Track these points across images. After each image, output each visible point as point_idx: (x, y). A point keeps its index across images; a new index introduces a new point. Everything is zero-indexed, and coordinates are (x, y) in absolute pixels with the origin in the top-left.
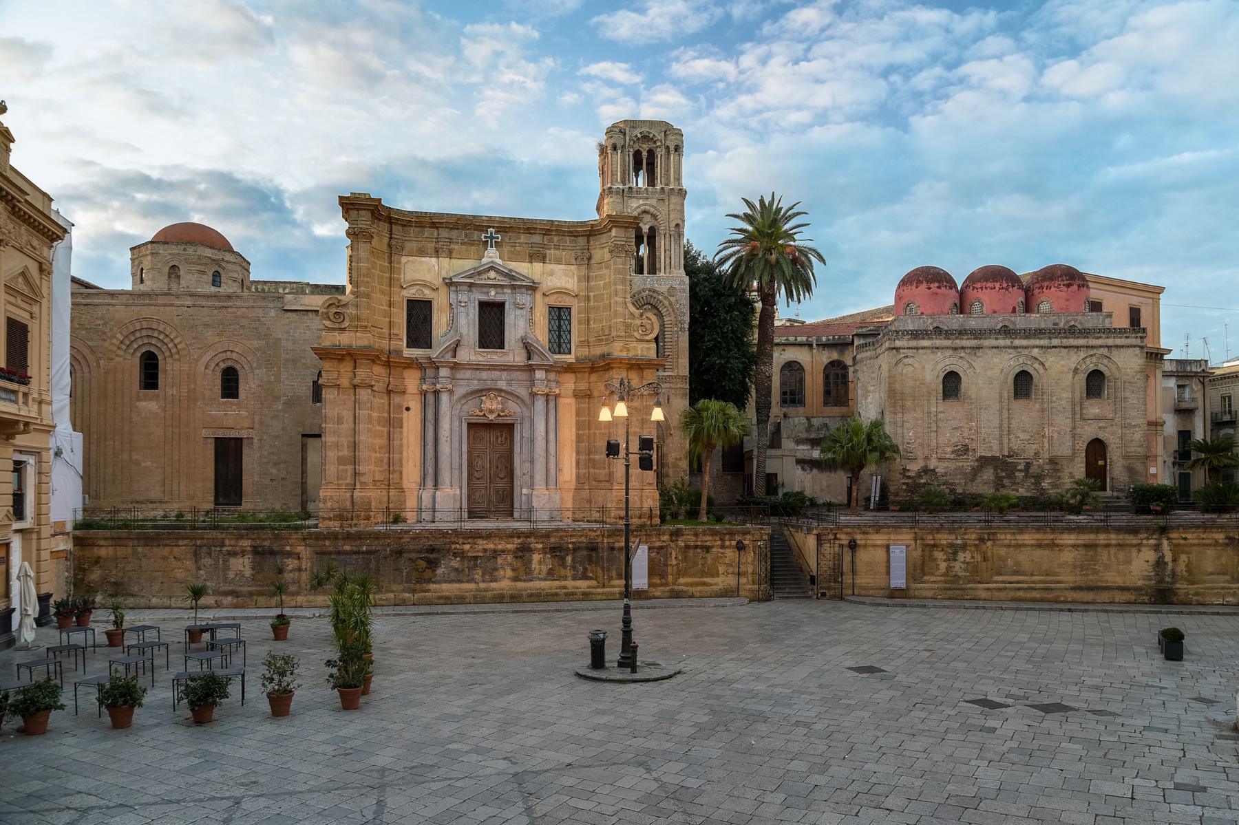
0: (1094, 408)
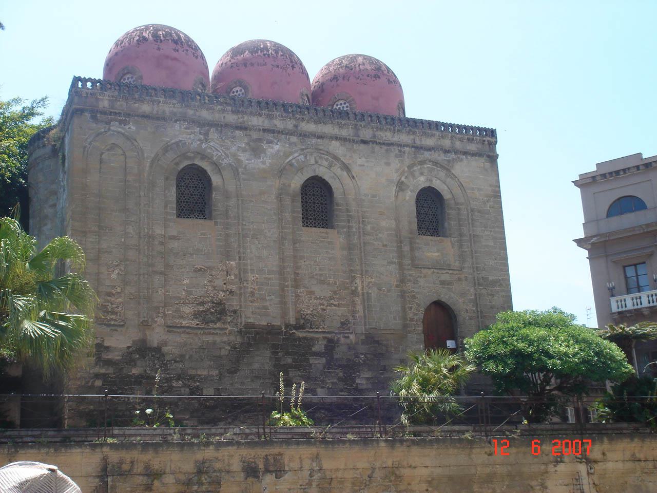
0: (431, 249)
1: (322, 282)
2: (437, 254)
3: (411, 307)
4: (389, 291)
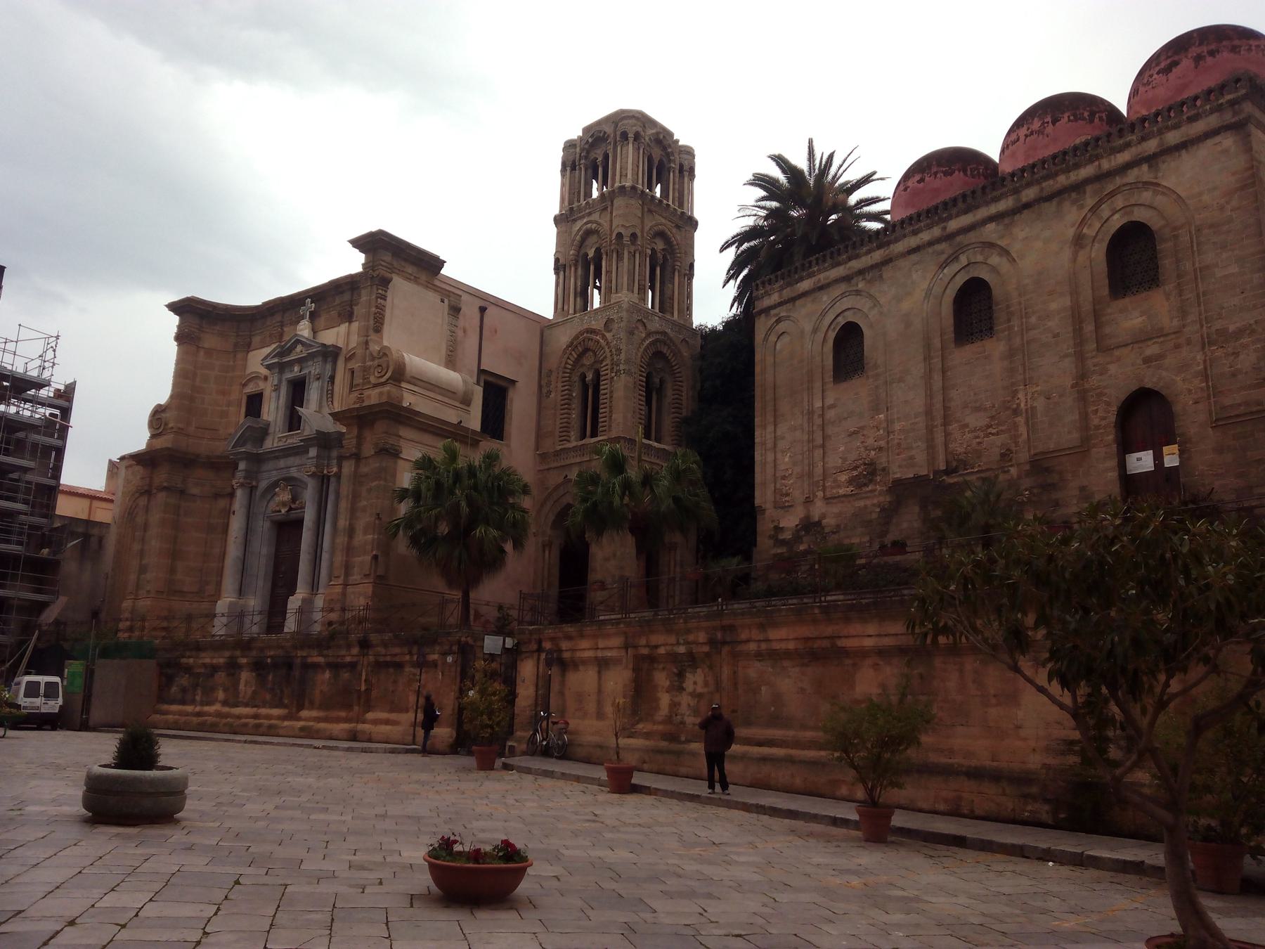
1: (978, 409)
2: (1140, 319)
3: (1097, 411)
4: (1061, 396)
